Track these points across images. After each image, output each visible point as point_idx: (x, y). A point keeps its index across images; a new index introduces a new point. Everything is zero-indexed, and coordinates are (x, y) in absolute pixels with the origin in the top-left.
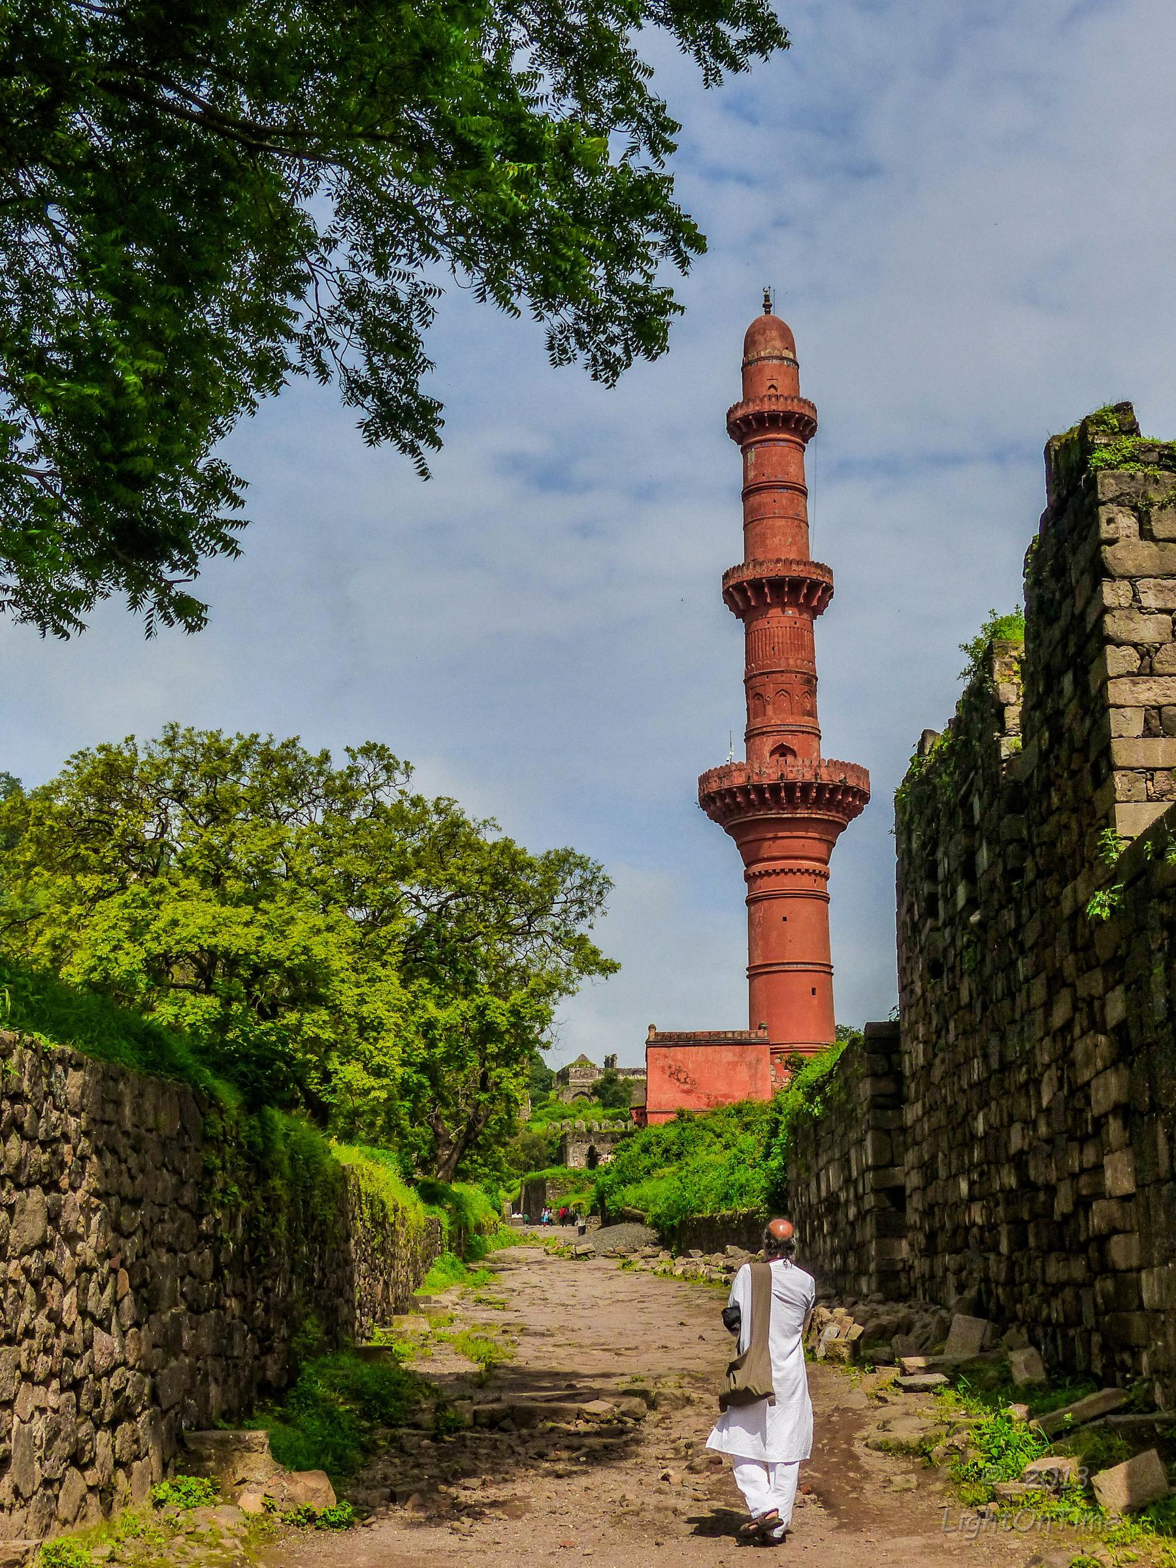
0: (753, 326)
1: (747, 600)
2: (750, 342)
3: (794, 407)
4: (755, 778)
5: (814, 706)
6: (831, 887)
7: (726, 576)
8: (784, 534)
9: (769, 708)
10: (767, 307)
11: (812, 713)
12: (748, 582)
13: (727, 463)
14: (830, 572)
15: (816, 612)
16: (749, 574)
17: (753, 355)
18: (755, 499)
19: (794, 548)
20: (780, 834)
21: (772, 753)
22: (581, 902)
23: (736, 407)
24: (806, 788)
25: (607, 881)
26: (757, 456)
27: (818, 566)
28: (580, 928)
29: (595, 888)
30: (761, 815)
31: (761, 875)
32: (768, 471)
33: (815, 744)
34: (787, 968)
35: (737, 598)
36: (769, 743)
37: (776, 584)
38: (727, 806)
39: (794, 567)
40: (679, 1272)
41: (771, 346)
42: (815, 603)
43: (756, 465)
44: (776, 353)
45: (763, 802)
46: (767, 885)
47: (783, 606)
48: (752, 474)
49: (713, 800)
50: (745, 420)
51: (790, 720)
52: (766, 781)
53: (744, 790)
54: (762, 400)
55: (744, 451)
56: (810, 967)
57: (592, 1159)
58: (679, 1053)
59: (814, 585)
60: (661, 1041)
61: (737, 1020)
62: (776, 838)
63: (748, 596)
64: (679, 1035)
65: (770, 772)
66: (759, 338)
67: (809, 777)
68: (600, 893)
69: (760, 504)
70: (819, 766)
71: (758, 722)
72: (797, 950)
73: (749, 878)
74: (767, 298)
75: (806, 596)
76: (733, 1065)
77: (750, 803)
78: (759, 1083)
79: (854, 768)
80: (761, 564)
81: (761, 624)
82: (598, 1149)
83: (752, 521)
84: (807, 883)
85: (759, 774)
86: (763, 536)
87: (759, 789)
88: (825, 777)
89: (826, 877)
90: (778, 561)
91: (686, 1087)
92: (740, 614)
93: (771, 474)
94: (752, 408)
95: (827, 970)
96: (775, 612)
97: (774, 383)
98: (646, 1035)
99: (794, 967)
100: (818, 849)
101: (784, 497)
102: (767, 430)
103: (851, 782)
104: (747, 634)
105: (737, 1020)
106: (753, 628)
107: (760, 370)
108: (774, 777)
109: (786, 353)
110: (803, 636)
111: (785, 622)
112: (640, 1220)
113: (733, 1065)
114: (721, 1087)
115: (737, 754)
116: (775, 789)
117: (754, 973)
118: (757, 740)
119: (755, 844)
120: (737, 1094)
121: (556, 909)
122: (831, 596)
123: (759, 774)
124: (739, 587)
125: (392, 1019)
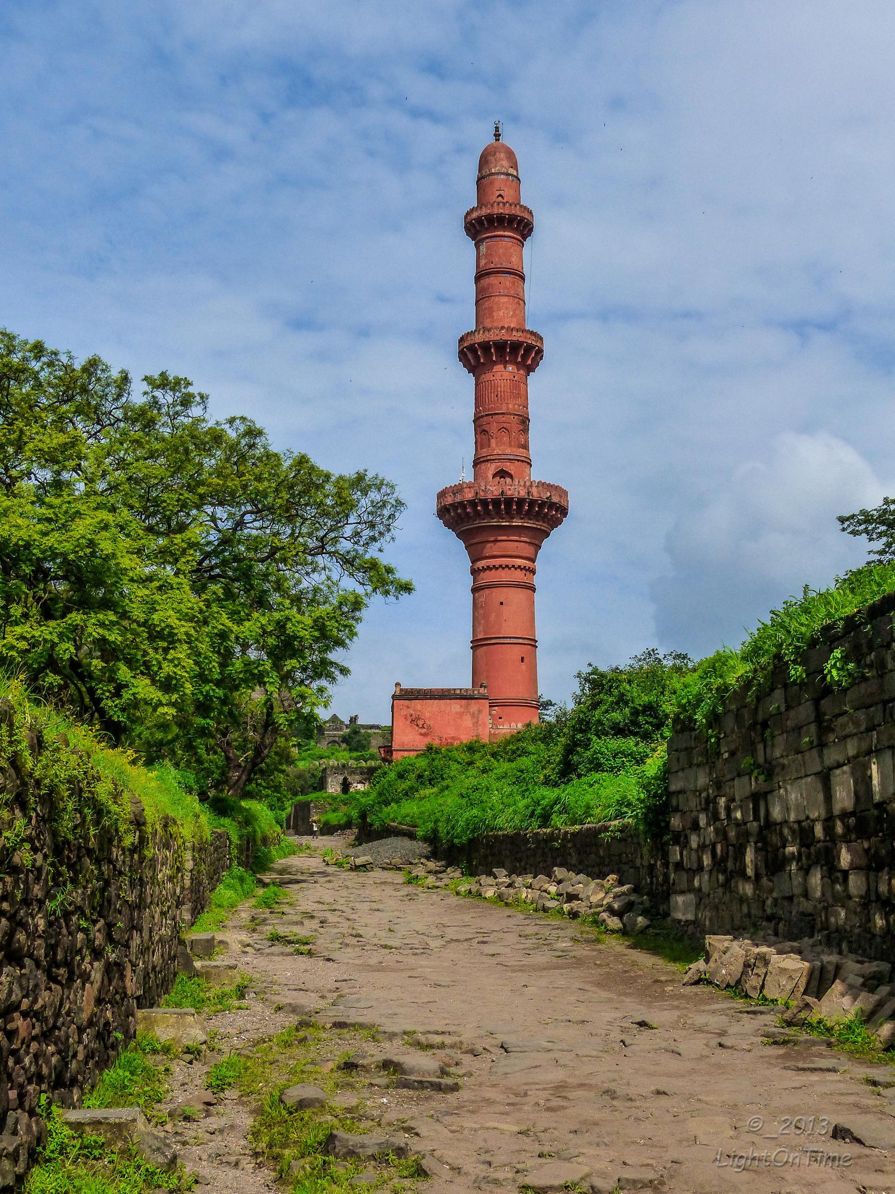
0: (486, 149)
1: (477, 358)
2: (484, 161)
3: (517, 211)
4: (482, 493)
5: (527, 441)
6: (537, 580)
7: (462, 340)
8: (507, 308)
9: (493, 441)
10: (497, 136)
11: (526, 447)
12: (480, 344)
13: (464, 255)
14: (541, 339)
15: (530, 369)
16: (479, 338)
17: (486, 172)
18: (485, 282)
19: (515, 320)
20: (500, 538)
21: (494, 476)
22: (372, 526)
23: (472, 210)
24: (521, 502)
25: (399, 503)
26: (488, 248)
27: (532, 333)
28: (372, 553)
29: (386, 512)
30: (485, 523)
31: (484, 569)
33: (527, 470)
34: (502, 641)
35: (470, 356)
36: (492, 468)
37: (500, 346)
38: (459, 515)
39: (514, 333)
40: (490, 893)
41: (500, 165)
42: (529, 362)
43: (486, 255)
44: (504, 170)
45: (487, 513)
46: (487, 577)
47: (505, 363)
48: (483, 262)
49: (448, 510)
50: (479, 220)
51: (508, 451)
52: (490, 496)
53: (473, 503)
54: (492, 205)
55: (477, 245)
56: (521, 641)
57: (346, 786)
58: (418, 704)
59: (529, 348)
60: (405, 695)
61: (463, 681)
62: (496, 541)
63: (477, 355)
64: (419, 691)
65: (493, 489)
66: (491, 159)
68: (391, 517)
69: (489, 285)
70: (531, 486)
71: (484, 452)
72: (510, 627)
73: (474, 572)
74: (497, 129)
75: (523, 356)
76: (461, 715)
77: (477, 514)
78: (480, 729)
79: (557, 488)
80: (489, 330)
81: (487, 377)
82: (350, 779)
83: (482, 297)
84: (519, 576)
85: (485, 491)
86: (491, 310)
87: (484, 503)
88: (535, 493)
89: (533, 572)
90: (503, 328)
91: (424, 731)
92: (472, 369)
93: (498, 262)
94: (484, 211)
95: (533, 643)
96: (499, 368)
97: (502, 192)
98: (392, 690)
99: (508, 641)
100: (528, 550)
101: (507, 280)
102: (496, 229)
103: (555, 499)
104: (477, 385)
105: (463, 681)
106: (481, 380)
107: (491, 183)
108: (496, 493)
109: (511, 171)
110: (519, 386)
111: (506, 375)
112: (411, 836)
113: (461, 715)
114: (450, 732)
115: (468, 476)
116: (496, 502)
117: (476, 644)
118: (483, 466)
119: (479, 546)
120: (462, 737)
121: (348, 531)
122: (541, 358)
123: (485, 491)
124: (472, 348)
125: (183, 628)
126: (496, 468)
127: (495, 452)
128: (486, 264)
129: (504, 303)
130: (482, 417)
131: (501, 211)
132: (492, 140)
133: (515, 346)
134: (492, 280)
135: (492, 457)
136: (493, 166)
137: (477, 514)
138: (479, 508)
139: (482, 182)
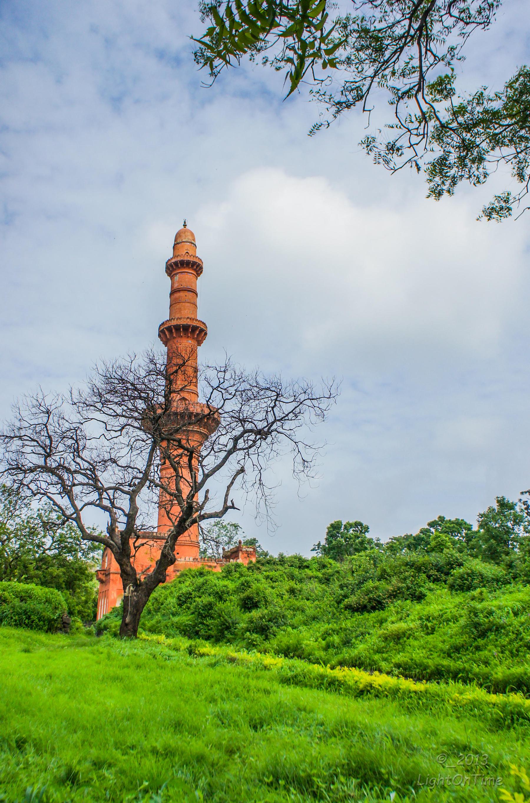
2: (178, 236)
10: (185, 226)
12: (174, 326)
16: (174, 323)
18: (177, 295)
23: (172, 259)
26: (179, 278)
35: (167, 333)
37: (186, 328)
50: (176, 263)
59: (202, 331)
66: (183, 235)
69: (179, 297)
74: (185, 222)
75: (198, 335)
86: (180, 309)
90: (188, 318)
93: (184, 285)
109: (193, 242)
124: (169, 329)
133: (195, 328)
134: (182, 294)
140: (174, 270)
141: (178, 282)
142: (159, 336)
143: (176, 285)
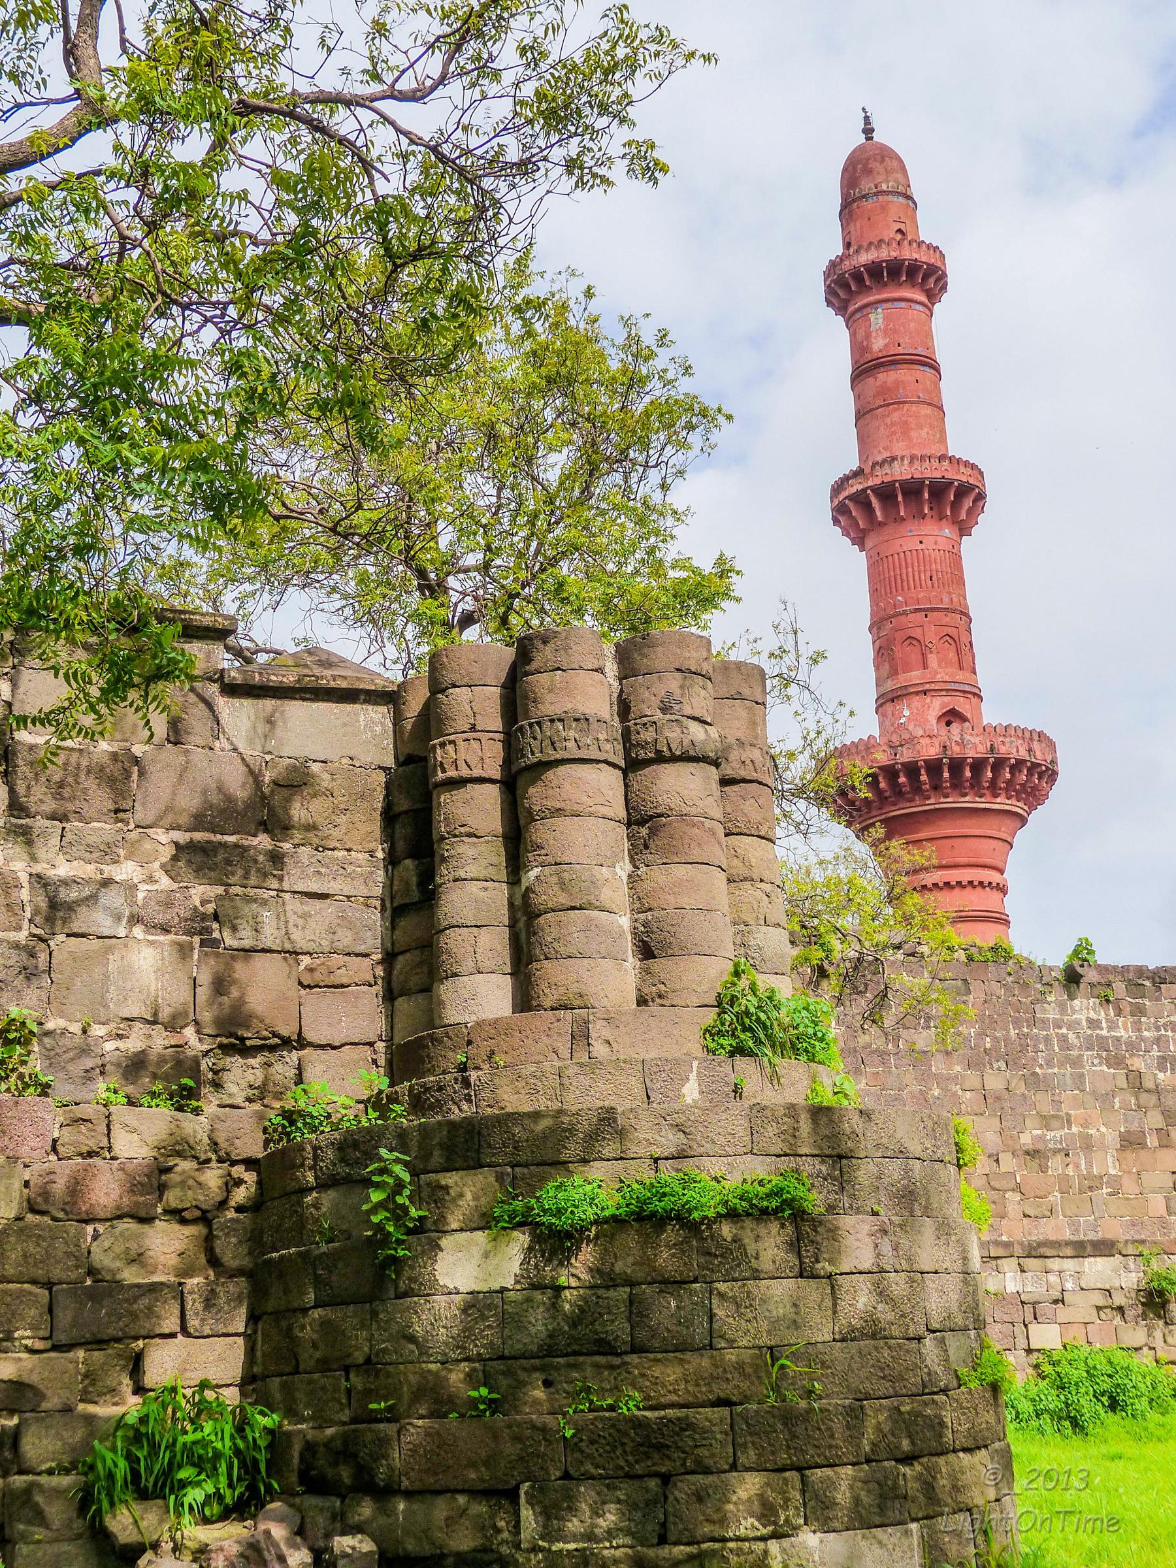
4: (956, 749)
9: (933, 660)
10: (868, 131)
12: (903, 483)
17: (867, 185)
26: (887, 318)
32: (905, 340)
37: (939, 489)
39: (962, 469)
45: (957, 785)
52: (971, 754)
53: (934, 767)
67: (1023, 754)
69: (897, 384)
74: (867, 118)
87: (956, 766)
97: (902, 226)
107: (884, 208)
108: (981, 748)
116: (978, 766)
126: (943, 705)
127: (939, 677)
128: (886, 346)
129: (926, 416)
130: (906, 613)
131: (915, 256)
132: (862, 139)
133: (964, 490)
135: (933, 686)
136: (870, 180)
137: (936, 787)
138: (902, 779)
139: (851, 206)
140: (863, 288)
141: (885, 332)
142: (840, 512)
143: (878, 344)
